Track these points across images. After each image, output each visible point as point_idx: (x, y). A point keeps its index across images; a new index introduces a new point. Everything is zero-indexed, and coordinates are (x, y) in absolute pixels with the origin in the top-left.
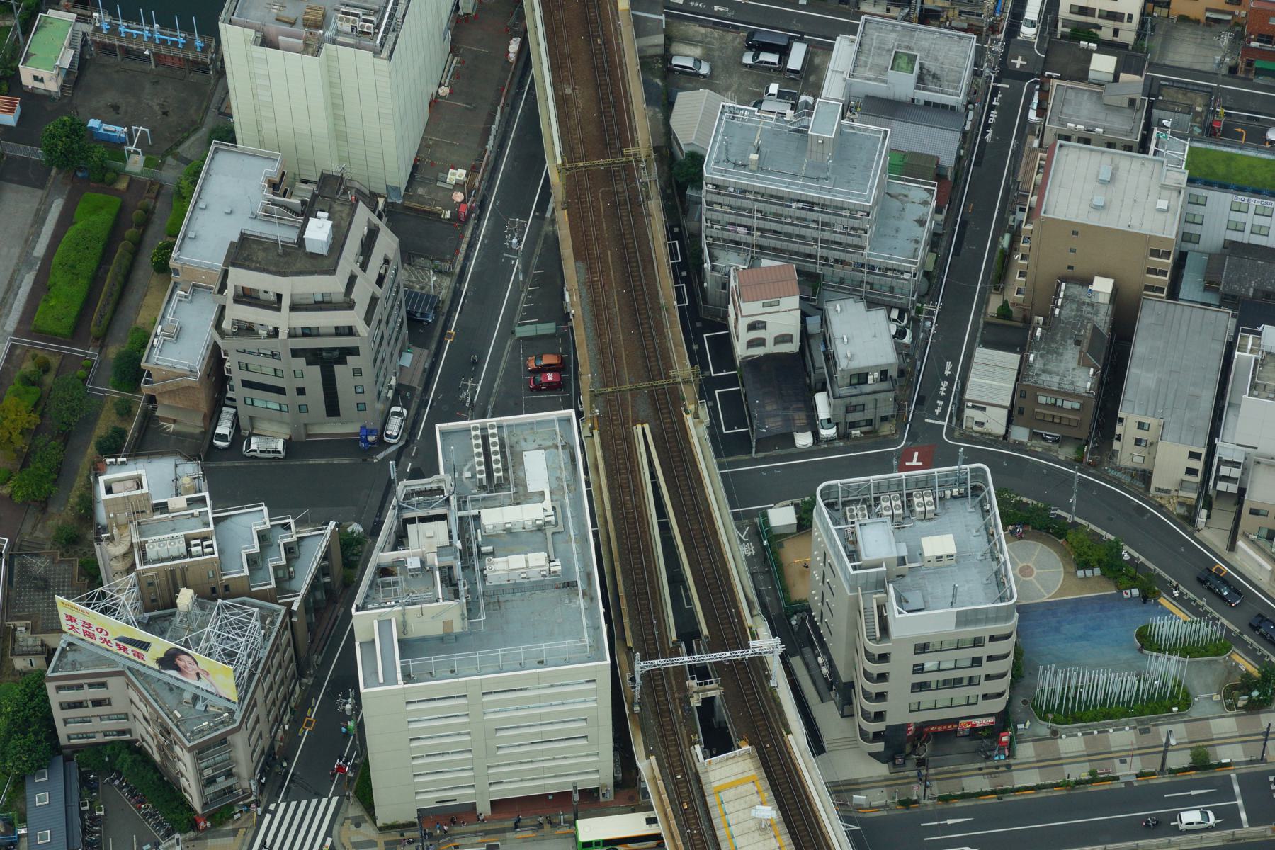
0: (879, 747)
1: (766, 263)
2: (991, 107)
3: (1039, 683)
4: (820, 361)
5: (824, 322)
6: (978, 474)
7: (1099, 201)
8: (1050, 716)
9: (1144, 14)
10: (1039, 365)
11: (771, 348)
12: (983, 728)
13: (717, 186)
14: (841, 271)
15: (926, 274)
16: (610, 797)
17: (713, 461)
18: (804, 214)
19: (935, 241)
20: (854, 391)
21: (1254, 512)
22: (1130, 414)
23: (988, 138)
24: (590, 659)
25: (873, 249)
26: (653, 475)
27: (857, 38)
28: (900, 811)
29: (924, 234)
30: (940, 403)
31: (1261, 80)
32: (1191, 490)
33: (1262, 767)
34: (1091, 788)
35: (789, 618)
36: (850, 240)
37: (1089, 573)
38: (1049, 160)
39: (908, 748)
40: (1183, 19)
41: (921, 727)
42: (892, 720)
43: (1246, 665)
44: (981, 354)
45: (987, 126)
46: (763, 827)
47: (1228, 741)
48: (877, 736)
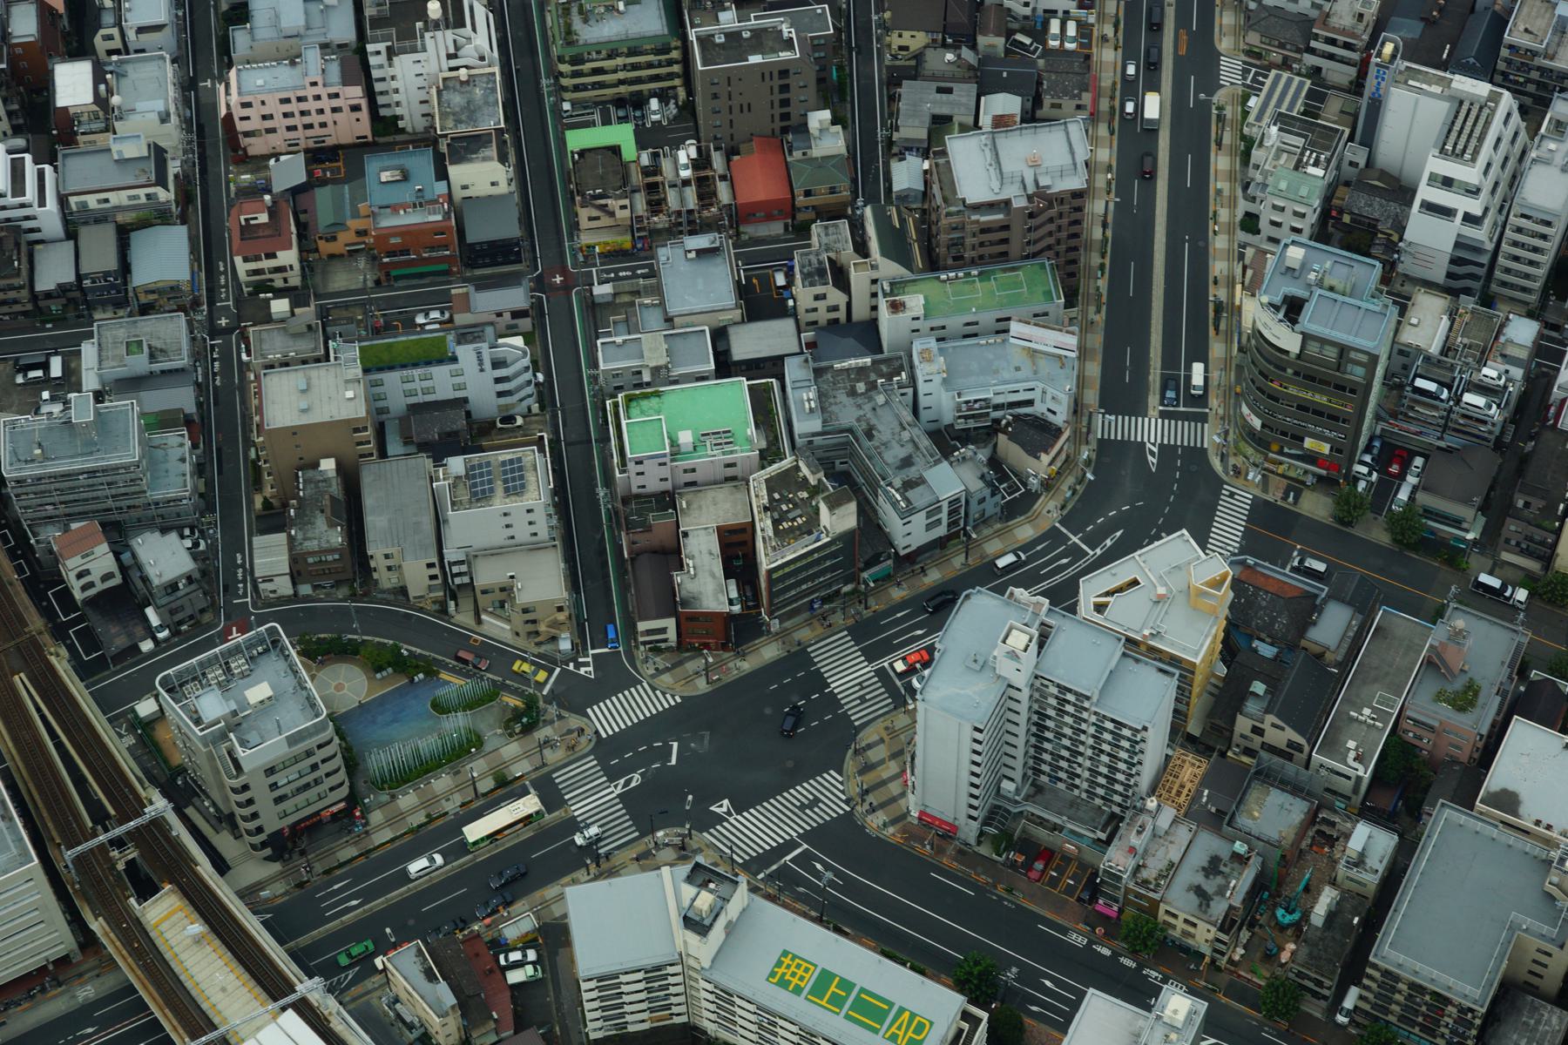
0: (268, 851)
1: (74, 526)
2: (214, 360)
3: (370, 765)
4: (139, 584)
5: (134, 556)
6: (272, 631)
7: (304, 405)
8: (386, 786)
9: (301, 260)
10: (300, 536)
11: (100, 587)
12: (340, 811)
13: (18, 482)
14: (134, 514)
15: (201, 495)
16: (79, 957)
17: (81, 685)
18: (91, 481)
19: (200, 469)
20: (172, 598)
21: (484, 592)
22: (376, 549)
23: (218, 383)
24: (22, 864)
25: (153, 490)
26: (38, 710)
27: (95, 340)
28: (298, 892)
29: (187, 468)
30: (241, 585)
31: (401, 283)
32: (439, 590)
33: (546, 770)
34: (430, 827)
35: (175, 780)
36: (133, 489)
37: (384, 673)
38: (259, 387)
39: (290, 845)
40: (332, 256)
41: (293, 826)
42: (269, 830)
43: (513, 701)
44: (258, 541)
45: (214, 374)
46: (198, 940)
47: (516, 759)
48: (264, 845)
